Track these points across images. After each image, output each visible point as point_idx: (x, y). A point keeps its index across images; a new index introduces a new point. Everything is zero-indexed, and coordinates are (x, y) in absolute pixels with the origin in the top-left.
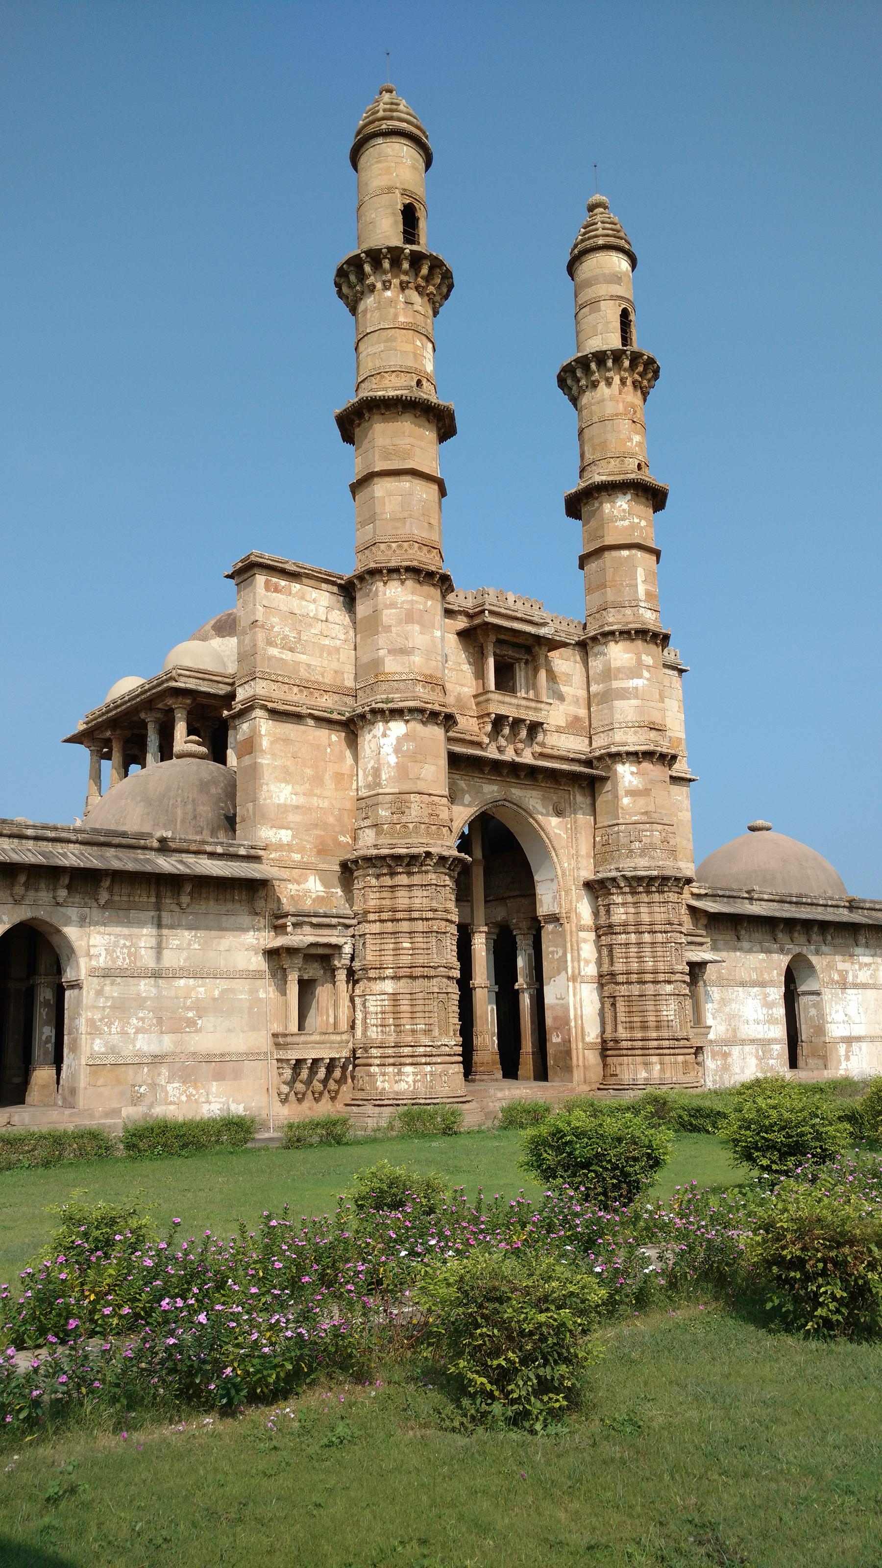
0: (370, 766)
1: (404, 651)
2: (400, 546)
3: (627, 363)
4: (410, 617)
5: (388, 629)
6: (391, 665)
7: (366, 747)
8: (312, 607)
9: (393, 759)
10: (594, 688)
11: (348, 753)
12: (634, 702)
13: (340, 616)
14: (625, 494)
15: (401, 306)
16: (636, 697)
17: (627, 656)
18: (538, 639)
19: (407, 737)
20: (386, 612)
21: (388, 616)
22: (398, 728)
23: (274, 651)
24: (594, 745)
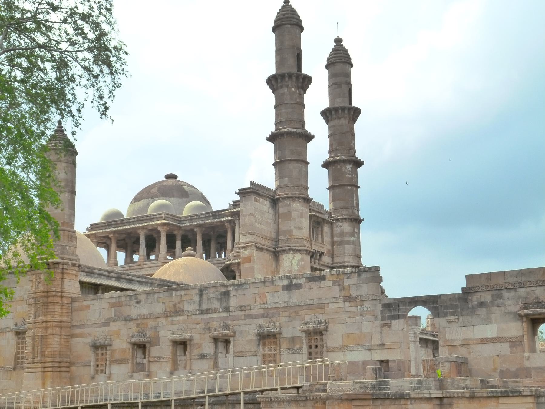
0: (286, 269)
1: (300, 228)
2: (298, 188)
3: (352, 112)
4: (302, 216)
5: (294, 219)
6: (295, 233)
7: (285, 262)
8: (265, 207)
9: (296, 268)
10: (336, 239)
11: (274, 263)
12: (352, 246)
13: (271, 211)
14: (350, 164)
15: (297, 95)
16: (353, 244)
17: (350, 228)
18: (323, 219)
19: (302, 260)
20: (293, 212)
21: (294, 214)
22: (298, 256)
23: (257, 224)
24: (335, 261)
